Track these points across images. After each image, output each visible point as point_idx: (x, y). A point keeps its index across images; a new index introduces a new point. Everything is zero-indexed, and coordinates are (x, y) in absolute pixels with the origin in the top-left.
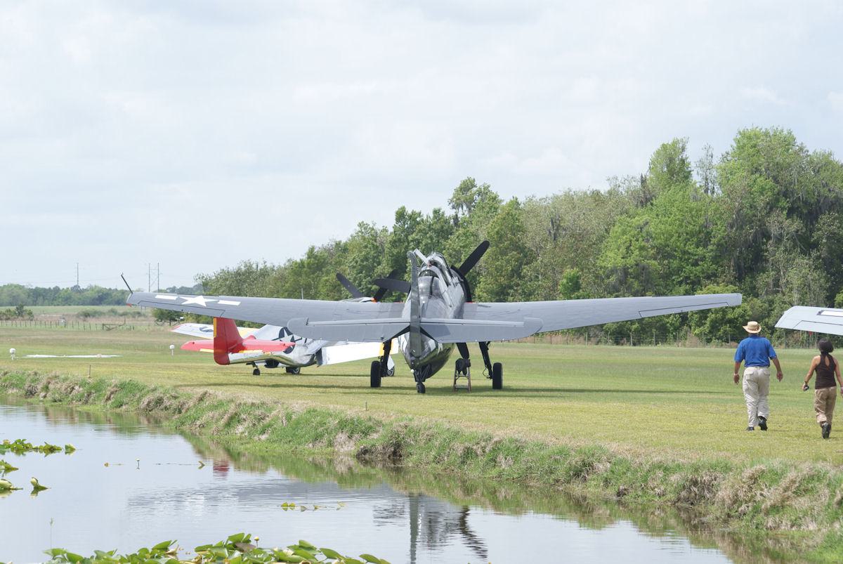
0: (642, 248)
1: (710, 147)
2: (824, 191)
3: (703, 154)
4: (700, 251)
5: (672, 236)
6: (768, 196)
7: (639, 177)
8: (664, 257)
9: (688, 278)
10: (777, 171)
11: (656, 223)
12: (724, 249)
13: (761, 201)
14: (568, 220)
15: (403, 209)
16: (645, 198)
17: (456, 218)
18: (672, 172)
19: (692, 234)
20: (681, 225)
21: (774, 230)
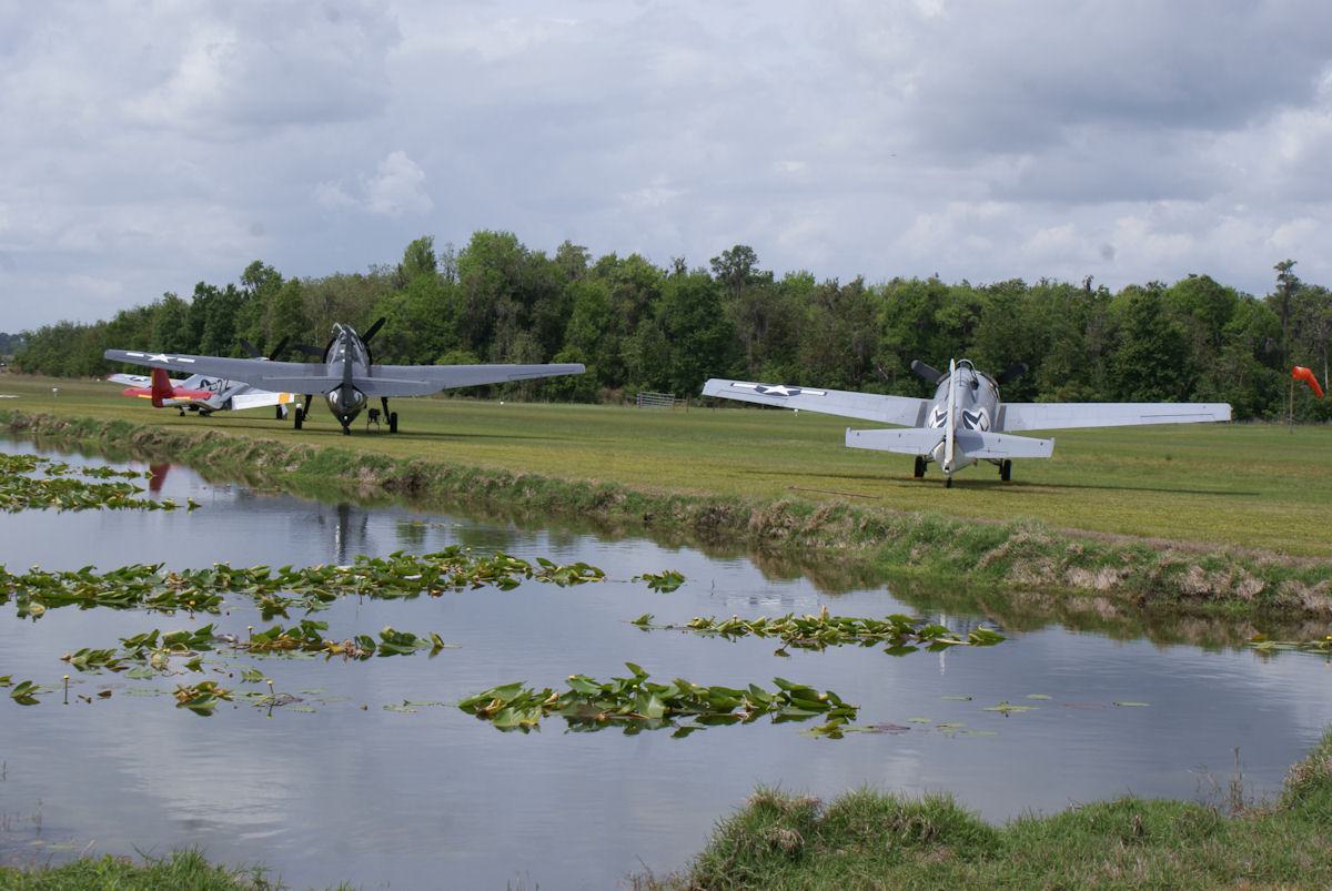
0: (400, 321)
1: (452, 242)
2: (539, 281)
3: (446, 249)
4: (446, 324)
5: (423, 313)
6: (497, 284)
7: (397, 266)
8: (416, 329)
9: (434, 346)
10: (504, 265)
11: (412, 303)
12: (463, 325)
13: (492, 287)
14: (340, 298)
15: (202, 283)
16: (401, 281)
17: (246, 293)
18: (421, 263)
19: (439, 311)
20: (431, 305)
21: (501, 309)
